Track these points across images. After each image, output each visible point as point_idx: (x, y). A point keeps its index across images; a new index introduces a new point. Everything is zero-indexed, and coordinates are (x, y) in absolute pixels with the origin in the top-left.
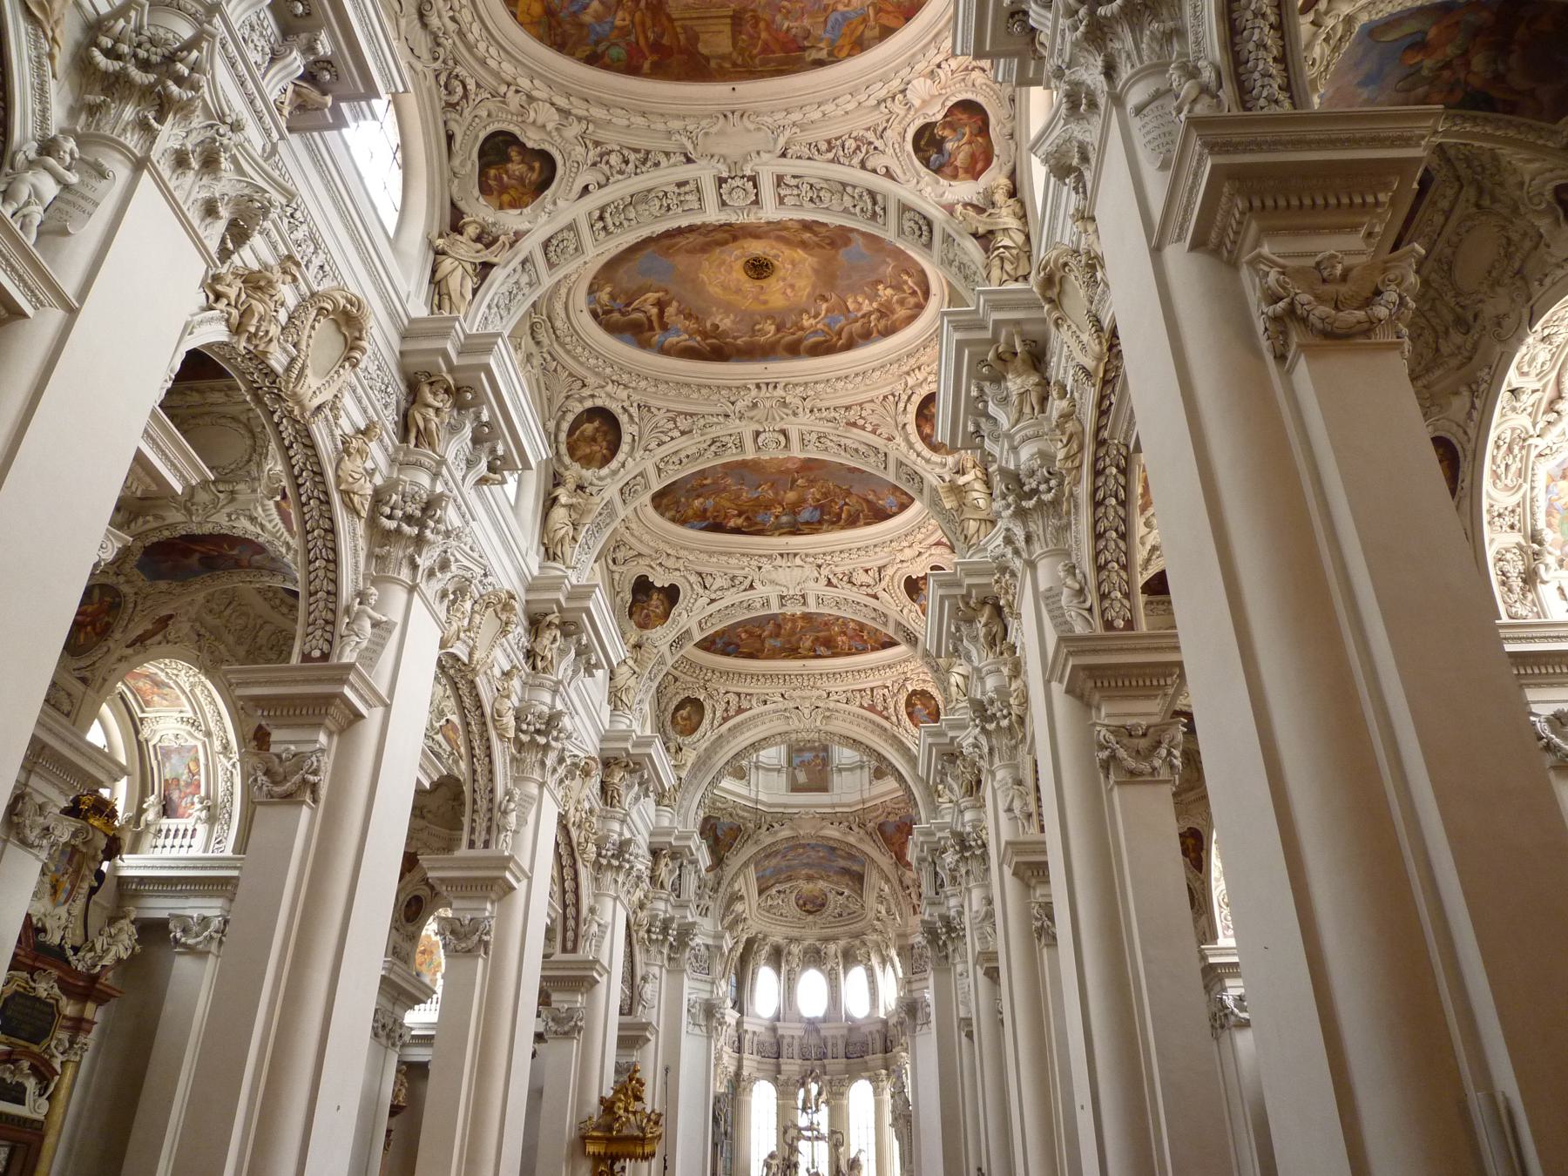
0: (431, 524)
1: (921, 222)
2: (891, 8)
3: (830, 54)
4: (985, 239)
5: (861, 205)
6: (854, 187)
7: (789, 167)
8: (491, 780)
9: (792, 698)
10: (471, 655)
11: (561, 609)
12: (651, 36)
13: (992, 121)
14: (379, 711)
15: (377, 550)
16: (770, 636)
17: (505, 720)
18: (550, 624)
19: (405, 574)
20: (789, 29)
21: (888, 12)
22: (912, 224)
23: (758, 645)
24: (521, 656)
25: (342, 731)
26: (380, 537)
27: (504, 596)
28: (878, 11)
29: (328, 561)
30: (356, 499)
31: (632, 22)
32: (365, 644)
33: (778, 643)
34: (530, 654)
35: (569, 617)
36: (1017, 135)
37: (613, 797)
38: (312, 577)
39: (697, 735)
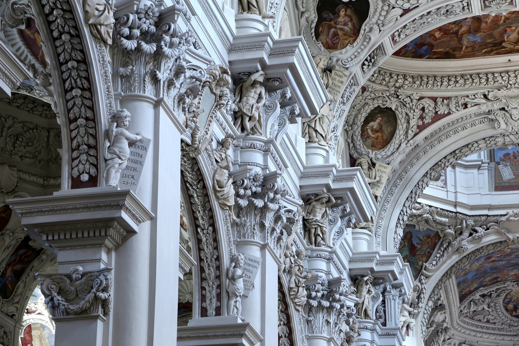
0: (167, 38)
8: (216, 248)
9: (497, 99)
10: (193, 136)
11: (264, 67)
14: (147, 225)
15: (122, 70)
16: (469, 32)
17: (226, 190)
18: (254, 84)
19: (149, 91)
23: (454, 43)
24: (230, 118)
25: (118, 247)
26: (123, 57)
27: (217, 73)
29: (83, 89)
30: (103, 29)
32: (125, 164)
33: (478, 38)
34: (238, 116)
35: (272, 73)
37: (316, 235)
38: (70, 104)
39: (391, 147)
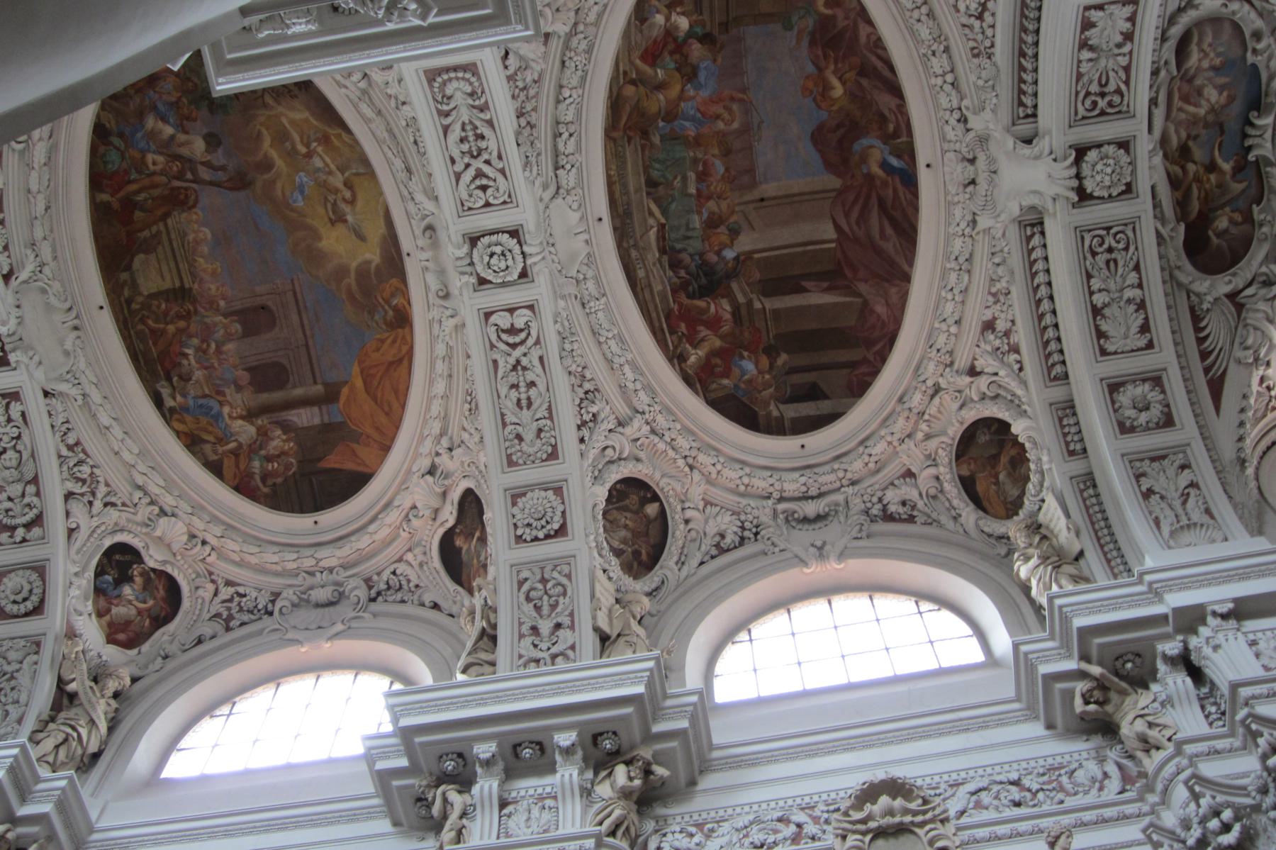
1: (35, 599)
2: (242, 467)
3: (172, 410)
4: (64, 698)
5: (17, 509)
6: (38, 494)
7: (34, 404)
12: (141, 197)
13: (171, 627)
20: (186, 356)
21: (237, 466)
22: (27, 587)
28: (235, 453)
31: (154, 173)
36: (171, 665)
